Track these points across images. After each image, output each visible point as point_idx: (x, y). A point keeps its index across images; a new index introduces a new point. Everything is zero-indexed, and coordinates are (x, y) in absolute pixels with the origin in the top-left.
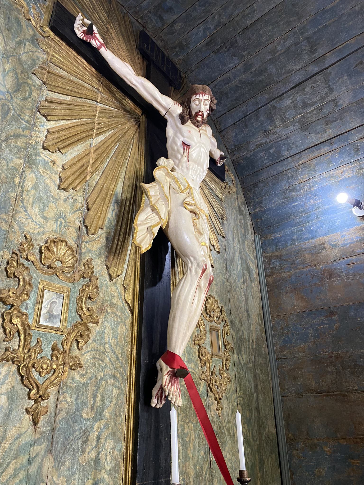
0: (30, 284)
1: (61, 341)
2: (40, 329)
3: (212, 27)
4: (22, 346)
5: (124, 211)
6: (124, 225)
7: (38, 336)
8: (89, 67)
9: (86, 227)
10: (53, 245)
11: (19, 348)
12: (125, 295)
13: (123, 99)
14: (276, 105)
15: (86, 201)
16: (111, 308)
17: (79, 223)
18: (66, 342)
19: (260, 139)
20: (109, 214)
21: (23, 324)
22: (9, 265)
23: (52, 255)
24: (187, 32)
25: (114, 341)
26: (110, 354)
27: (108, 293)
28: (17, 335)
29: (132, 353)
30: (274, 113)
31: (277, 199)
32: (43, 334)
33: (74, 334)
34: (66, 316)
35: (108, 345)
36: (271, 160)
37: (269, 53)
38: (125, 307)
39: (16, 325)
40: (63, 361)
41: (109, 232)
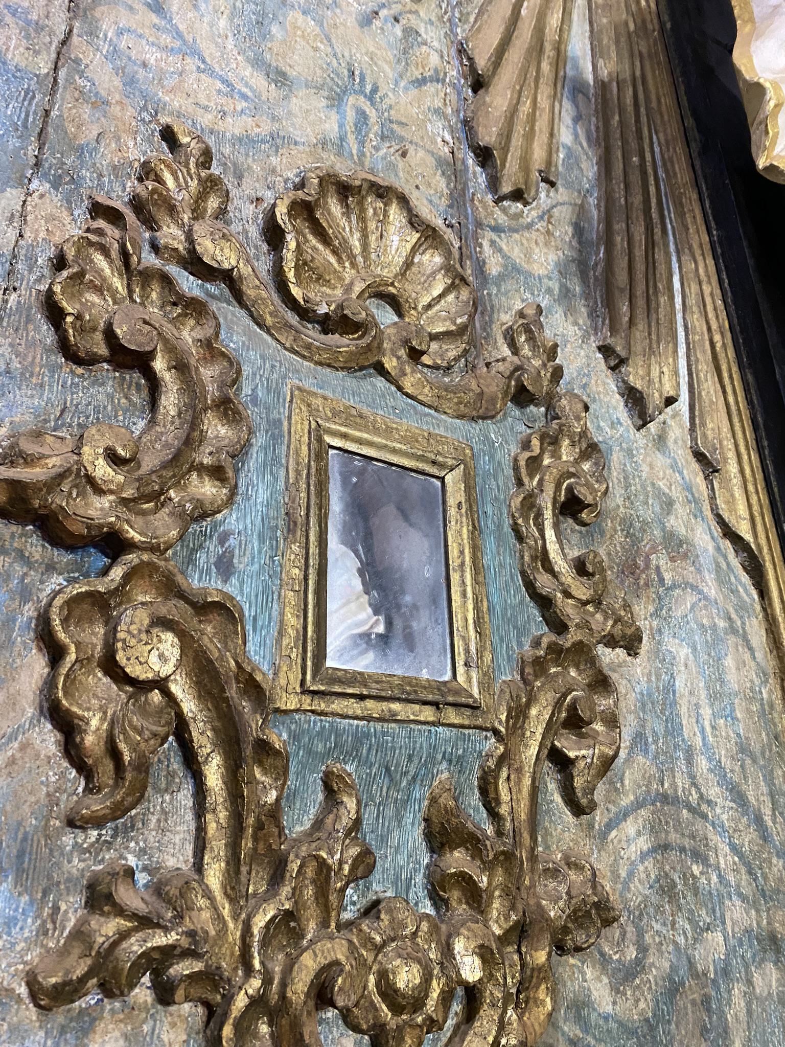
0: (227, 407)
1: (477, 774)
2: (338, 705)
4: (218, 845)
5: (621, 122)
6: (635, 177)
7: (328, 753)
9: (484, 156)
10: (335, 208)
11: (199, 867)
12: (713, 498)
16: (673, 559)
17: (448, 138)
18: (504, 774)
20: (563, 129)
22: (65, 273)
23: (340, 260)
25: (728, 738)
26: (723, 810)
27: (644, 487)
28: (176, 765)
32: (360, 738)
33: (539, 715)
34: (477, 608)
35: (702, 764)
38: (725, 557)
39: (161, 684)
40: (513, 907)
41: (582, 206)
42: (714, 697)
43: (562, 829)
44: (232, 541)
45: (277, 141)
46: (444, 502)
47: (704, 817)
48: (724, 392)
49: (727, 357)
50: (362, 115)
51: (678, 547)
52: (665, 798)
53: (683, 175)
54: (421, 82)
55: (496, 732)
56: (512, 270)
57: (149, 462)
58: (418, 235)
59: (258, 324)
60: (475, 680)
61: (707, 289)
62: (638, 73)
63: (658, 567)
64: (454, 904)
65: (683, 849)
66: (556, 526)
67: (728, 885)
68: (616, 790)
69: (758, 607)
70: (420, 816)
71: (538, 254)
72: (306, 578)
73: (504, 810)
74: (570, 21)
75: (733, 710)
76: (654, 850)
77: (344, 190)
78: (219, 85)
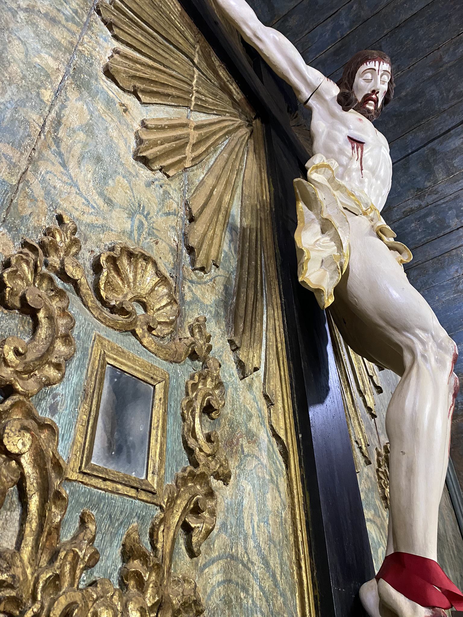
0: (67, 339)
1: (149, 526)
2: (94, 481)
3: (346, 24)
4: (29, 540)
6: (252, 270)
7: (86, 503)
8: (180, 9)
9: (191, 250)
10: (125, 261)
11: (18, 547)
12: (270, 417)
13: (228, 81)
14: (437, 148)
15: (186, 204)
16: (249, 442)
17: (176, 239)
18: (162, 528)
19: (409, 202)
20: (225, 244)
21: (39, 457)
22: (10, 270)
23: (123, 283)
24: (307, 32)
25: (264, 532)
26: (258, 569)
28: (15, 498)
29: (300, 568)
30: (435, 161)
31: (443, 293)
32: (101, 498)
33: (181, 503)
35: (251, 543)
36: (430, 234)
37: (430, 66)
38: (273, 447)
39: (17, 457)
41: (229, 278)
42: (260, 512)
43: (183, 563)
44: (58, 398)
45: (104, 228)
46: (154, 397)
47: (249, 569)
48: (280, 370)
49: (283, 354)
50: (141, 223)
51: (252, 437)
52: (232, 557)
53: (273, 272)
54: (168, 214)
55: (161, 507)
56: (196, 300)
57: (30, 357)
58: (159, 279)
59: (85, 305)
60: (155, 481)
61: (277, 324)
62: (259, 227)
63: (242, 445)
64: (130, 587)
65: (237, 584)
66: (200, 417)
67: (256, 606)
68: (210, 548)
69: (285, 473)
70: (121, 542)
71: (207, 295)
72: (88, 421)
73: (159, 546)
74: (233, 199)
75: (268, 520)
76: (224, 582)
77: (131, 255)
78: (84, 200)
